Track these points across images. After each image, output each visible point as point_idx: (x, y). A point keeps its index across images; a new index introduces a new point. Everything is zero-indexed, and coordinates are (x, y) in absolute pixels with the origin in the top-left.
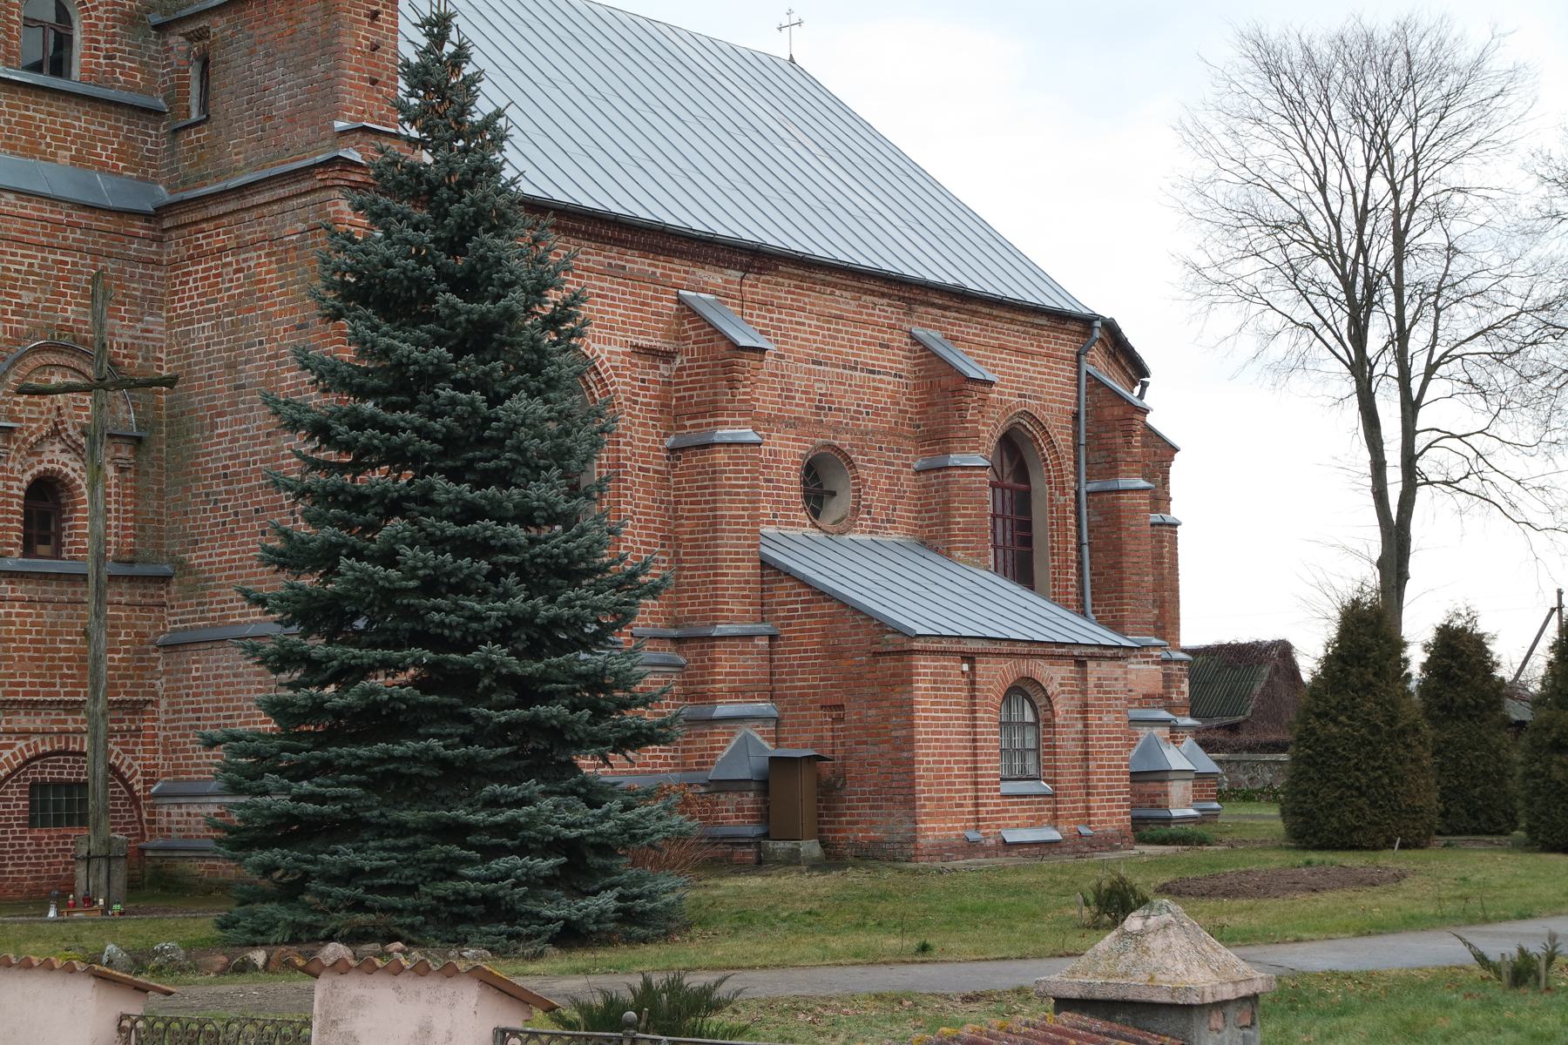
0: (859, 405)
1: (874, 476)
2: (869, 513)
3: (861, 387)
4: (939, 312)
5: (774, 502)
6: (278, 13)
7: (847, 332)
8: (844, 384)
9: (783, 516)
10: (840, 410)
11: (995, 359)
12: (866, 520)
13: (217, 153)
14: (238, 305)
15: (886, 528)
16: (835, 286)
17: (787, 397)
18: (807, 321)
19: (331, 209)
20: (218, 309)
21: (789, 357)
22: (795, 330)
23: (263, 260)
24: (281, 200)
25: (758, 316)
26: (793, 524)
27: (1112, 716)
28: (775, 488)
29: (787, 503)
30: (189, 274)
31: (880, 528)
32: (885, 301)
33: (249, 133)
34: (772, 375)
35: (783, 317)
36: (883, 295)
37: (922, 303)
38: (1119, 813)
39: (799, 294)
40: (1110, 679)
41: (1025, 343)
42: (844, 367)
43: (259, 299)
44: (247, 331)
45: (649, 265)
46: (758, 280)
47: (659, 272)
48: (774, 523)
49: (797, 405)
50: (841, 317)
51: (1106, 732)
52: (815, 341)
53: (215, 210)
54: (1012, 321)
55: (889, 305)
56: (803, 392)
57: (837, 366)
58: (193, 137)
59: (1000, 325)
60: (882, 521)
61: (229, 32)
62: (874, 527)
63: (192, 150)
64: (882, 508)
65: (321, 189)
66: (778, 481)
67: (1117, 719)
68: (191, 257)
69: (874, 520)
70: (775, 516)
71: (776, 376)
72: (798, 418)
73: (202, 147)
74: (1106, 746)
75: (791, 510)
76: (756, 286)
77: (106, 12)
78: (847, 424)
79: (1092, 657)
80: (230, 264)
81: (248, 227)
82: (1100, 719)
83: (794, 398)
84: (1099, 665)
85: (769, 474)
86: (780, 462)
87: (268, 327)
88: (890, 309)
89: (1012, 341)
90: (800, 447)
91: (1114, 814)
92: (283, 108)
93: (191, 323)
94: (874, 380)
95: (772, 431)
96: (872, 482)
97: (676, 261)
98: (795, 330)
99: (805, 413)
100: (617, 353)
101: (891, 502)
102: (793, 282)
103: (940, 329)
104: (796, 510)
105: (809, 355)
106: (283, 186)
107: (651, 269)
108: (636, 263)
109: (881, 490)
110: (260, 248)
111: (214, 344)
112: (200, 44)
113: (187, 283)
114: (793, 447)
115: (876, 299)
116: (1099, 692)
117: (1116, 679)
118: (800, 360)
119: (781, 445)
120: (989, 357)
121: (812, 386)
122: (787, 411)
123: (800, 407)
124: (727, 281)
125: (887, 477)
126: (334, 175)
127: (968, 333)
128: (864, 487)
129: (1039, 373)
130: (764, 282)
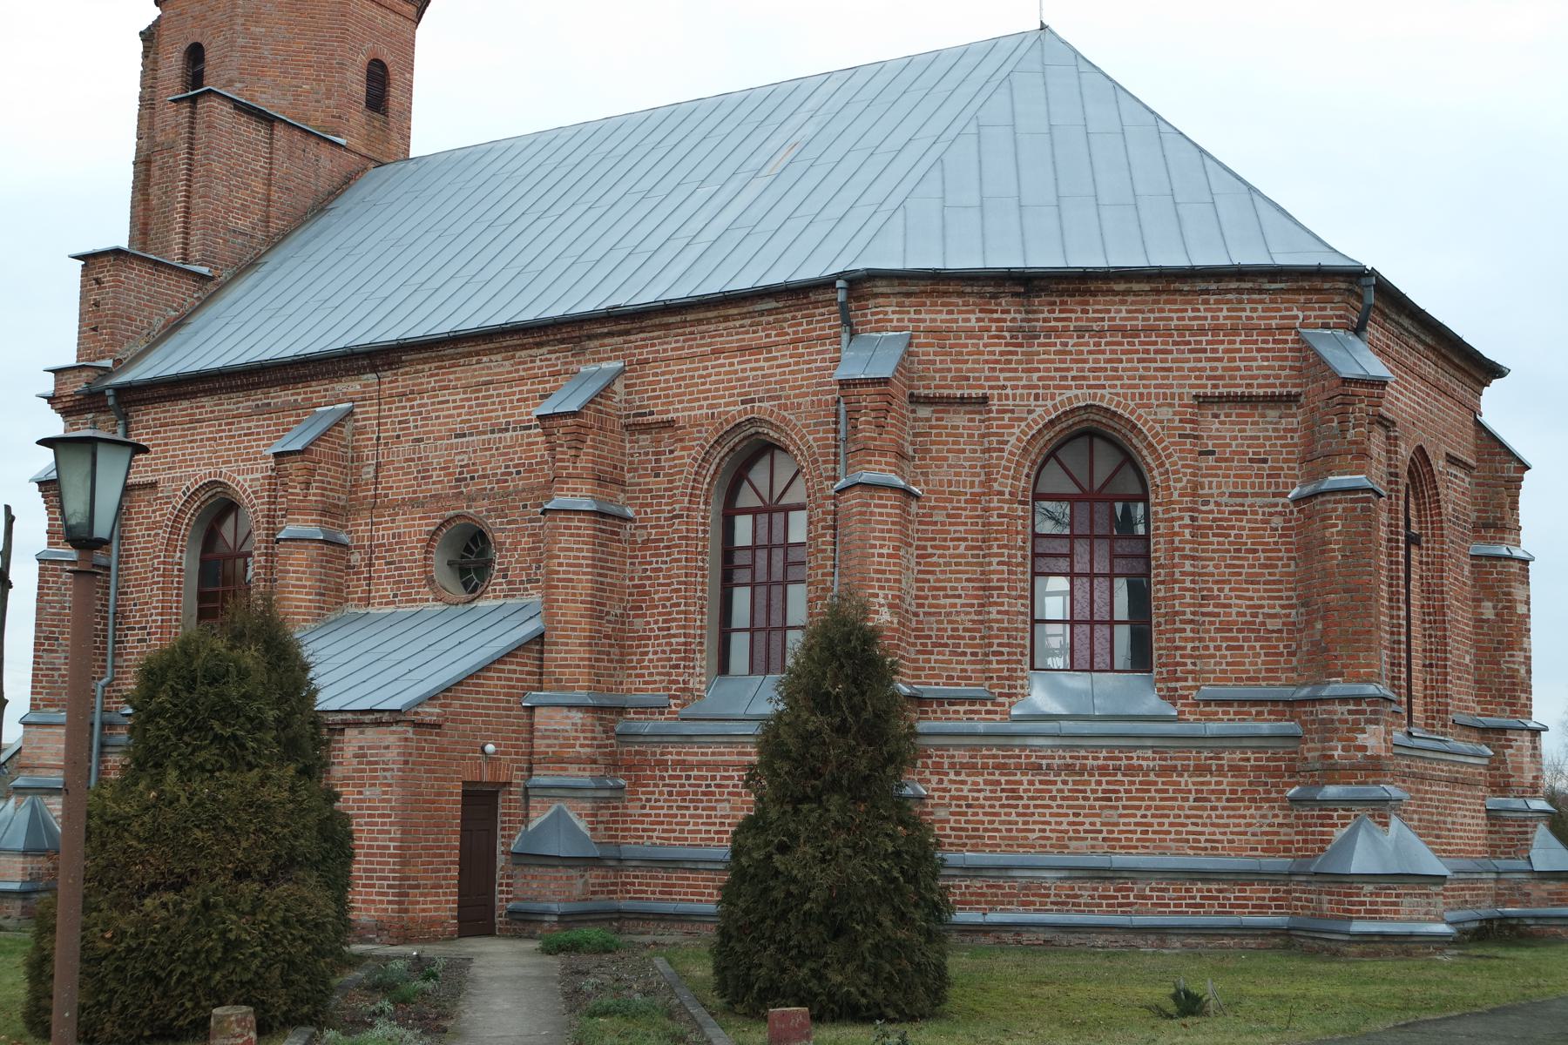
0: (507, 467)
1: (514, 537)
2: (505, 576)
3: (510, 447)
4: (620, 339)
5: (395, 583)
7: (499, 396)
8: (491, 449)
9: (402, 595)
10: (484, 476)
11: (706, 368)
12: (501, 584)
15: (526, 589)
16: (477, 354)
17: (423, 478)
18: (451, 398)
21: (429, 438)
22: (437, 410)
25: (397, 408)
26: (415, 600)
27: (378, 790)
28: (396, 569)
29: (410, 582)
31: (519, 590)
32: (545, 350)
34: (407, 460)
35: (425, 401)
36: (539, 345)
37: (590, 337)
38: (381, 902)
39: (443, 374)
40: (379, 748)
41: (748, 338)
42: (493, 432)
45: (292, 395)
46: (396, 374)
47: (300, 398)
48: (394, 603)
49: (434, 483)
50: (491, 382)
51: (368, 808)
52: (459, 415)
54: (726, 319)
55: (550, 352)
56: (441, 469)
57: (484, 433)
59: (712, 327)
60: (522, 582)
62: (510, 590)
64: (522, 569)
66: (401, 562)
67: (385, 793)
69: (509, 583)
70: (395, 596)
71: (412, 460)
72: (434, 496)
74: (367, 824)
75: (413, 587)
76: (397, 381)
78: (492, 489)
79: (347, 724)
82: (360, 793)
83: (431, 477)
84: (361, 733)
85: (391, 556)
86: (405, 543)
88: (554, 356)
89: (733, 341)
90: (427, 525)
91: (373, 902)
94: (529, 436)
95: (397, 514)
96: (511, 544)
97: (314, 383)
98: (437, 410)
99: (443, 489)
100: (258, 479)
101: (533, 561)
102: (433, 365)
103: (624, 357)
104: (419, 587)
105: (450, 430)
107: (292, 398)
108: (280, 397)
109: (523, 549)
114: (419, 525)
115: (534, 352)
116: (359, 763)
117: (387, 748)
118: (441, 438)
119: (405, 527)
120: (697, 369)
121: (453, 461)
122: (422, 492)
123: (439, 483)
124: (365, 386)
125: (529, 535)
127: (665, 351)
128: (501, 551)
129: (779, 366)
130: (402, 374)
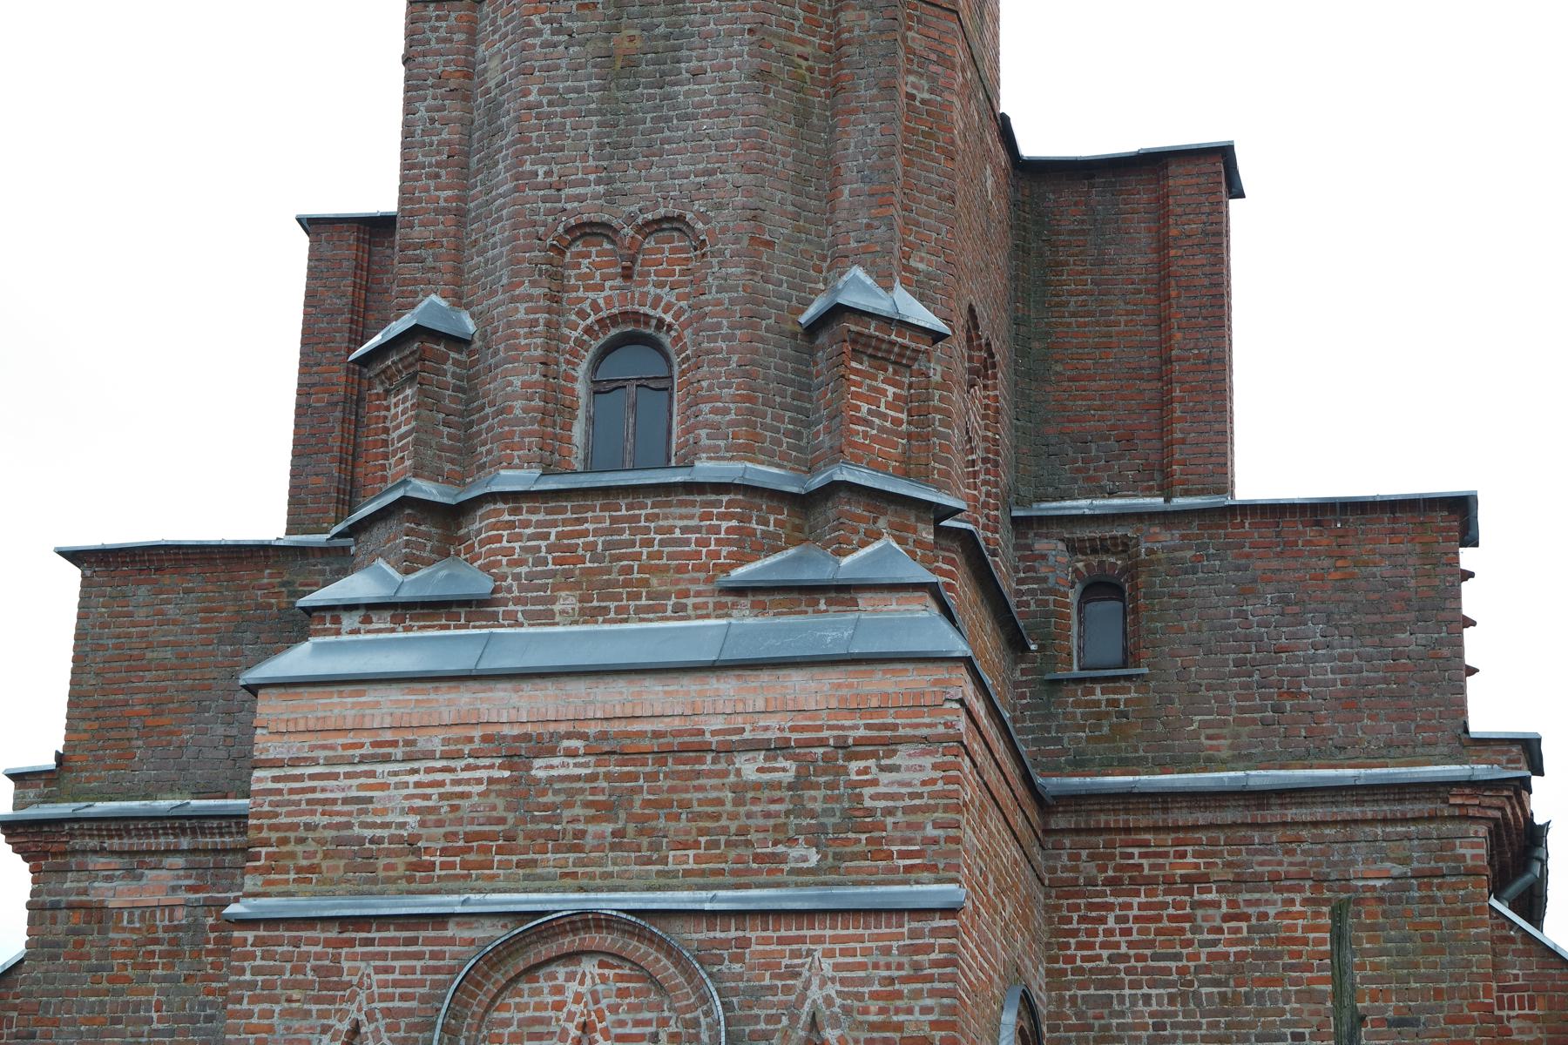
6: (1307, 543)
13: (1159, 728)
14: (1236, 970)
19: (1468, 852)
20: (1182, 971)
23: (1298, 908)
24: (1345, 823)
30: (1109, 907)
33: (1242, 710)
43: (1286, 967)
44: (1260, 1013)
53: (1182, 817)
58: (1098, 695)
61: (1189, 554)
63: (1100, 716)
65: (1452, 818)
68: (1109, 882)
73: (1124, 715)
77: (985, 483)
80: (1216, 904)
81: (1257, 852)
87: (1317, 1013)
92: (1326, 684)
93: (1118, 985)
106: (1360, 803)
110: (1290, 889)
111: (1175, 1026)
112: (1094, 560)
113: (1103, 920)
126: (1496, 802)
